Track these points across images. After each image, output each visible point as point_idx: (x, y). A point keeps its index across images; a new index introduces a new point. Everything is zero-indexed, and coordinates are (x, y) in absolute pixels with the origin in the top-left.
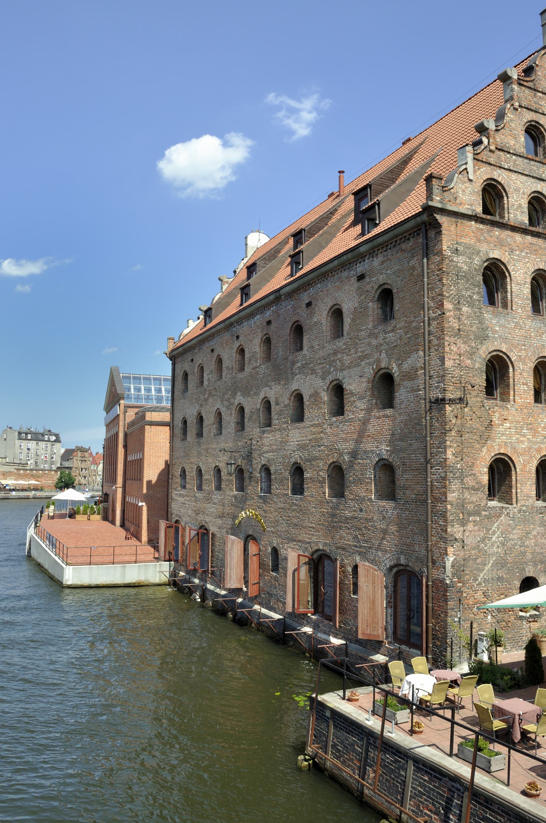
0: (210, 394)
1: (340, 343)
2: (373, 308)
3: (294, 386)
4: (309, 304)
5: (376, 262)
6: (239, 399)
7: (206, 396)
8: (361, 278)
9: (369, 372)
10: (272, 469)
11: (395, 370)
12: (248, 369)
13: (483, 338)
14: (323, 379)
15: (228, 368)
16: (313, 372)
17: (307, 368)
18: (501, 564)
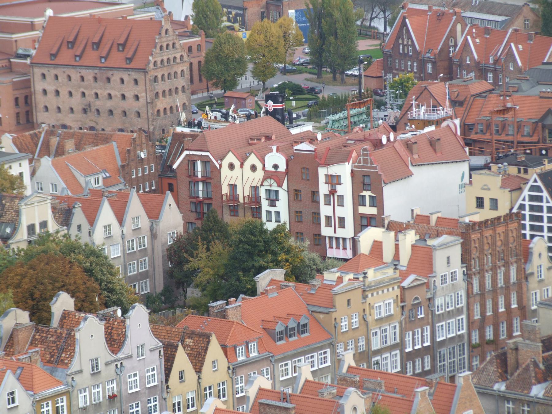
2: (133, 82)
3: (108, 91)
4: (112, 75)
5: (133, 73)
6: (82, 90)
8: (129, 75)
9: (133, 94)
10: (100, 110)
11: (139, 95)
12: (86, 83)
13: (154, 90)
14: (119, 92)
15: (75, 80)
16: (115, 90)
17: (111, 88)
18: (159, 127)
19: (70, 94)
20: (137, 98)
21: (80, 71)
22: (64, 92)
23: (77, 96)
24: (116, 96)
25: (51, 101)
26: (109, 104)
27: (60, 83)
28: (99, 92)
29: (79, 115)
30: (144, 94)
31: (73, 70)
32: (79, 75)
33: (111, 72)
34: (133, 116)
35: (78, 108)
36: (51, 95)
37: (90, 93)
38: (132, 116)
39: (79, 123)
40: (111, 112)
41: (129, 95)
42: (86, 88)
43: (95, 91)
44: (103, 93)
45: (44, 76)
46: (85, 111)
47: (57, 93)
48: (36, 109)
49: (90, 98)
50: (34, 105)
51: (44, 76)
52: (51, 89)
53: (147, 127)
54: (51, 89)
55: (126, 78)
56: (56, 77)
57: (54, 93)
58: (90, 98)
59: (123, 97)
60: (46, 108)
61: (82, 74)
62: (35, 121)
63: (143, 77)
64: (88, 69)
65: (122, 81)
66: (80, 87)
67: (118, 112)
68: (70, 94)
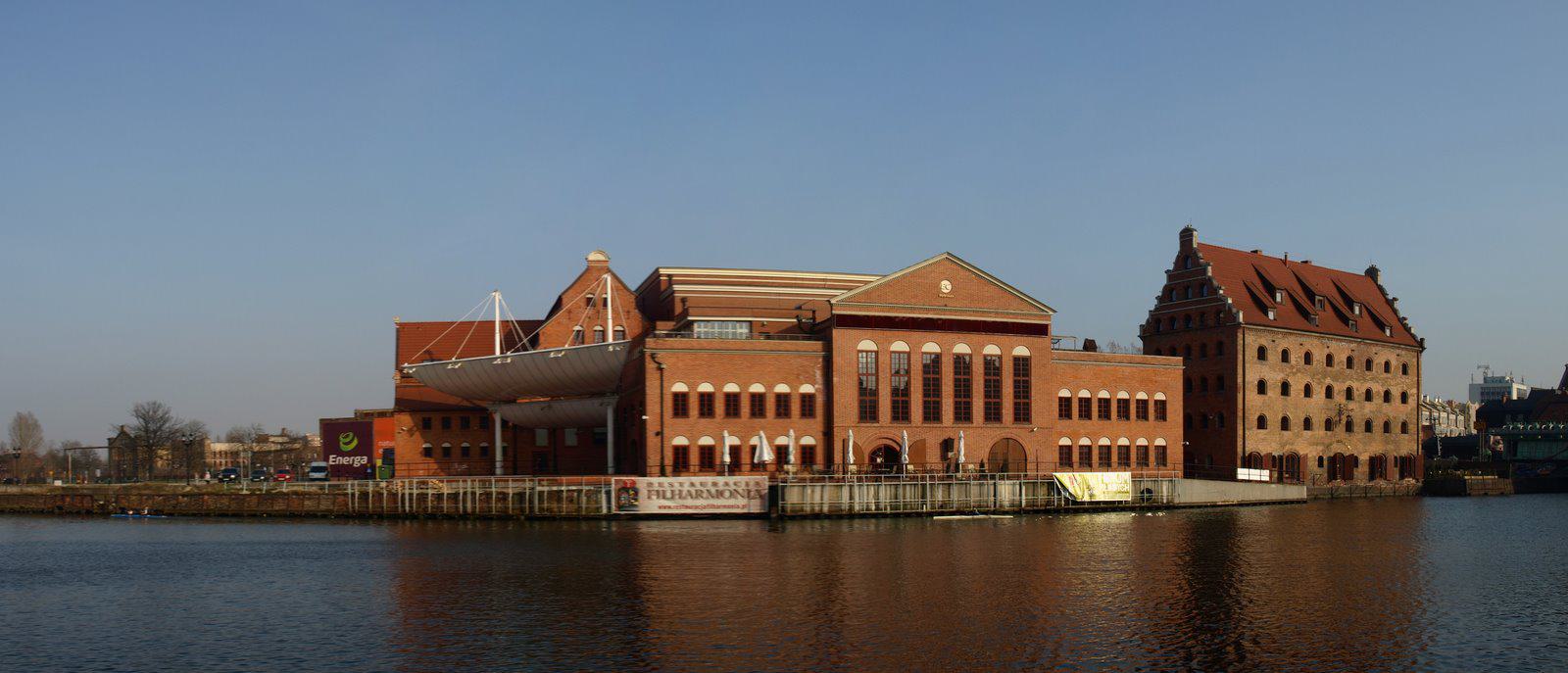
0: (1298, 371)
1: (1389, 375)
6: (1328, 381)
7: (1294, 370)
9: (1400, 390)
12: (1336, 368)
19: (1308, 391)
20: (1404, 397)
21: (1329, 343)
22: (1297, 387)
23: (1319, 394)
24: (1378, 392)
25: (1272, 405)
26: (1369, 409)
27: (1292, 367)
28: (1355, 385)
29: (1319, 431)
30: (1415, 391)
31: (1316, 341)
32: (1326, 351)
33: (1374, 349)
34: (1398, 429)
35: (1318, 420)
36: (1274, 392)
37: (1339, 388)
38: (1396, 429)
39: (1320, 448)
40: (1368, 427)
41: (1396, 393)
42: (1335, 379)
43: (1348, 383)
44: (1359, 389)
45: (1262, 353)
46: (1329, 425)
47: (1285, 389)
48: (1244, 422)
49: (1339, 398)
50: (1240, 414)
51: (1262, 353)
52: (1274, 376)
53: (1416, 448)
54: (1274, 376)
55: (1393, 363)
56: (1285, 356)
57: (1279, 390)
58: (1339, 398)
59: (1387, 397)
60: (1262, 423)
61: (1331, 350)
62: (1240, 450)
63: (1415, 360)
64: (1341, 341)
65: (1387, 365)
66: (1325, 377)
67: (1378, 425)
68: (1308, 391)
